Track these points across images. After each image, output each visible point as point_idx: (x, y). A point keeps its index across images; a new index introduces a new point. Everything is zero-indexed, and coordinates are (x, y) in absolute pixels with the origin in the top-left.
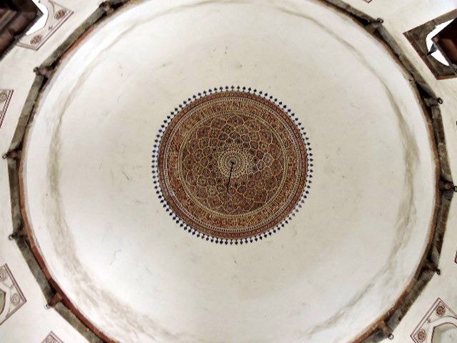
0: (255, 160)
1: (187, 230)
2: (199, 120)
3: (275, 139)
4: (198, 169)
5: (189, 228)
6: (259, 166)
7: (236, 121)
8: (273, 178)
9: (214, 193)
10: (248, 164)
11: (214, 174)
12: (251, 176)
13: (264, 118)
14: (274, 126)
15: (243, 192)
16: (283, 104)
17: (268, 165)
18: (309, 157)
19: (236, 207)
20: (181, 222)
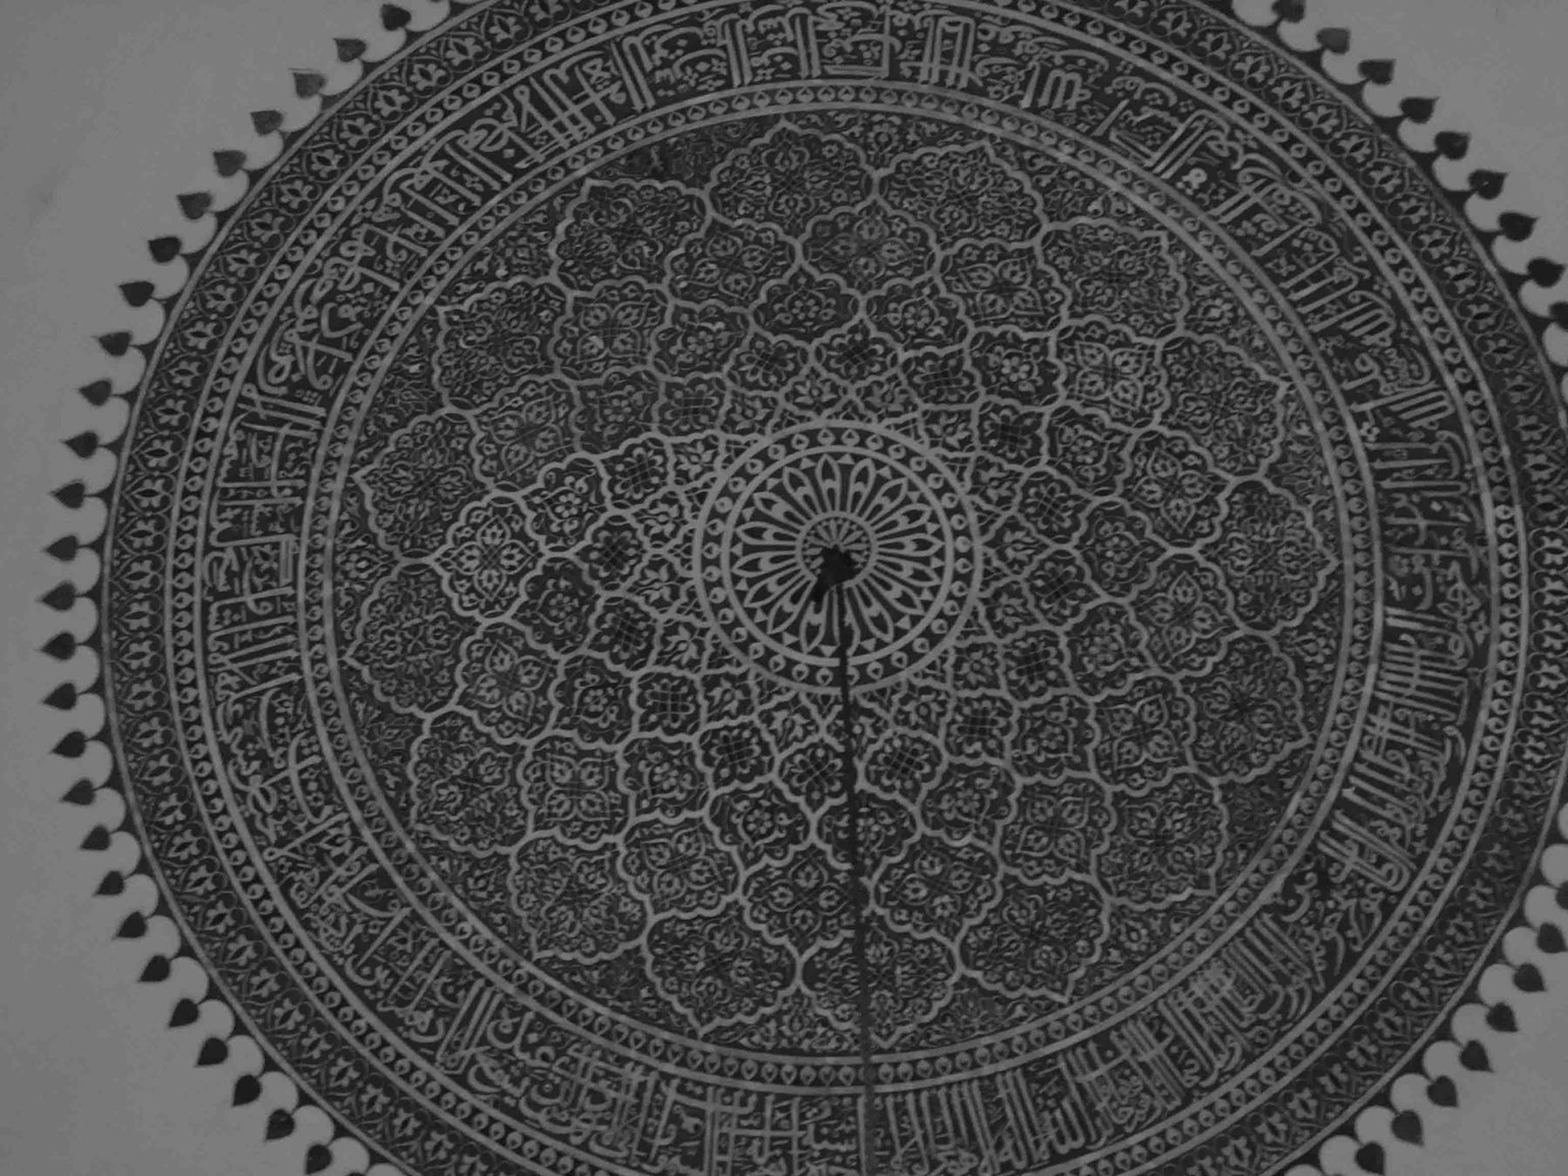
0: (615, 554)
1: (1475, 160)
2: (1039, 1074)
3: (388, 757)
4: (1183, 614)
5: (1452, 174)
6: (590, 507)
7: (718, 965)
8: (469, 388)
9: (1095, 354)
10: (699, 525)
11: (1046, 510)
12: (691, 410)
13: (458, 973)
14: (379, 890)
15: (801, 286)
16: (257, 1113)
17: (503, 513)
18: (82, 619)
19: (908, 183)
20: (1513, 255)
